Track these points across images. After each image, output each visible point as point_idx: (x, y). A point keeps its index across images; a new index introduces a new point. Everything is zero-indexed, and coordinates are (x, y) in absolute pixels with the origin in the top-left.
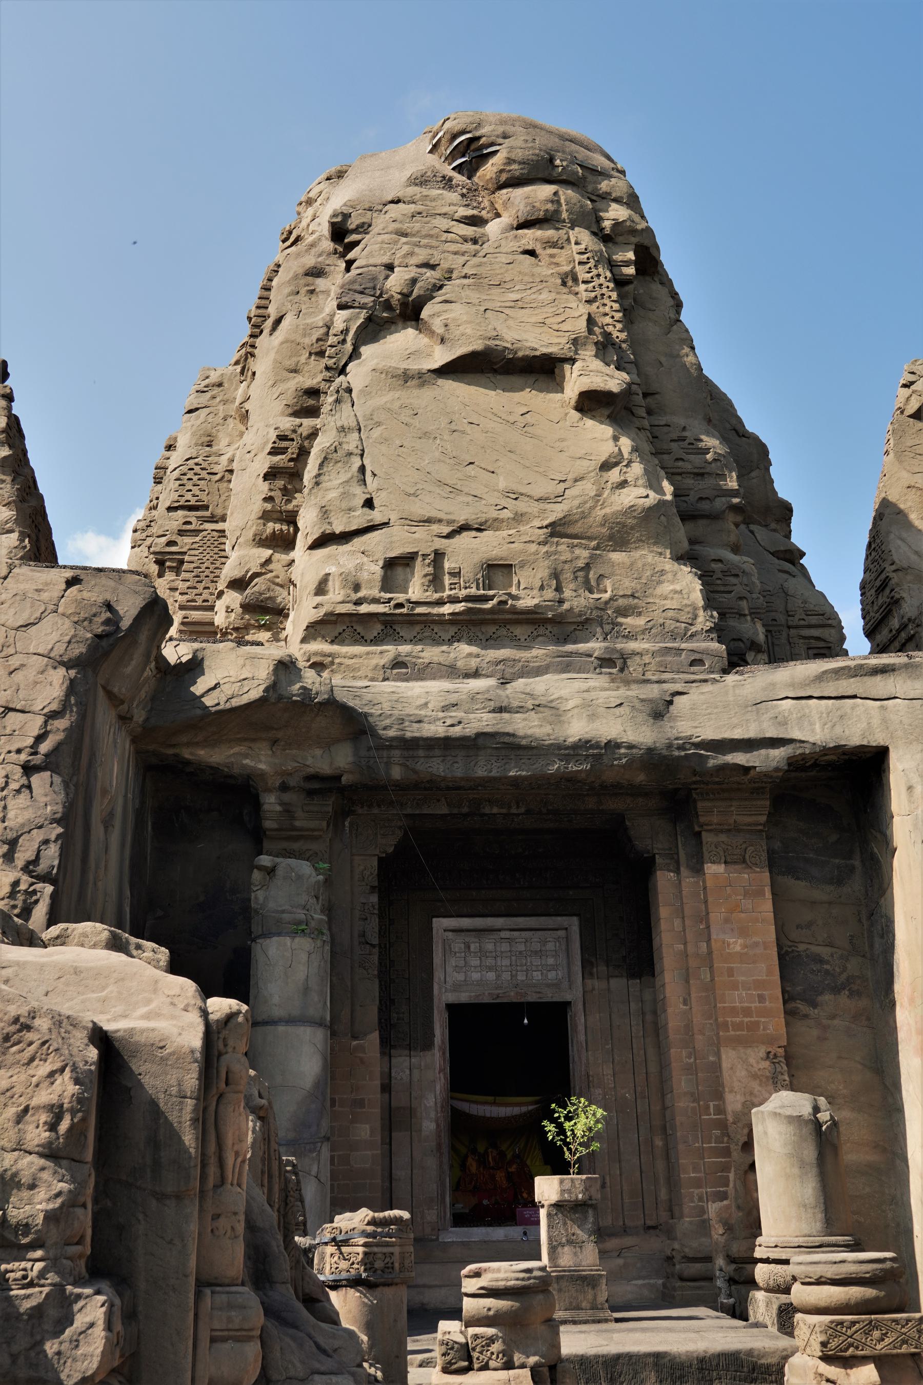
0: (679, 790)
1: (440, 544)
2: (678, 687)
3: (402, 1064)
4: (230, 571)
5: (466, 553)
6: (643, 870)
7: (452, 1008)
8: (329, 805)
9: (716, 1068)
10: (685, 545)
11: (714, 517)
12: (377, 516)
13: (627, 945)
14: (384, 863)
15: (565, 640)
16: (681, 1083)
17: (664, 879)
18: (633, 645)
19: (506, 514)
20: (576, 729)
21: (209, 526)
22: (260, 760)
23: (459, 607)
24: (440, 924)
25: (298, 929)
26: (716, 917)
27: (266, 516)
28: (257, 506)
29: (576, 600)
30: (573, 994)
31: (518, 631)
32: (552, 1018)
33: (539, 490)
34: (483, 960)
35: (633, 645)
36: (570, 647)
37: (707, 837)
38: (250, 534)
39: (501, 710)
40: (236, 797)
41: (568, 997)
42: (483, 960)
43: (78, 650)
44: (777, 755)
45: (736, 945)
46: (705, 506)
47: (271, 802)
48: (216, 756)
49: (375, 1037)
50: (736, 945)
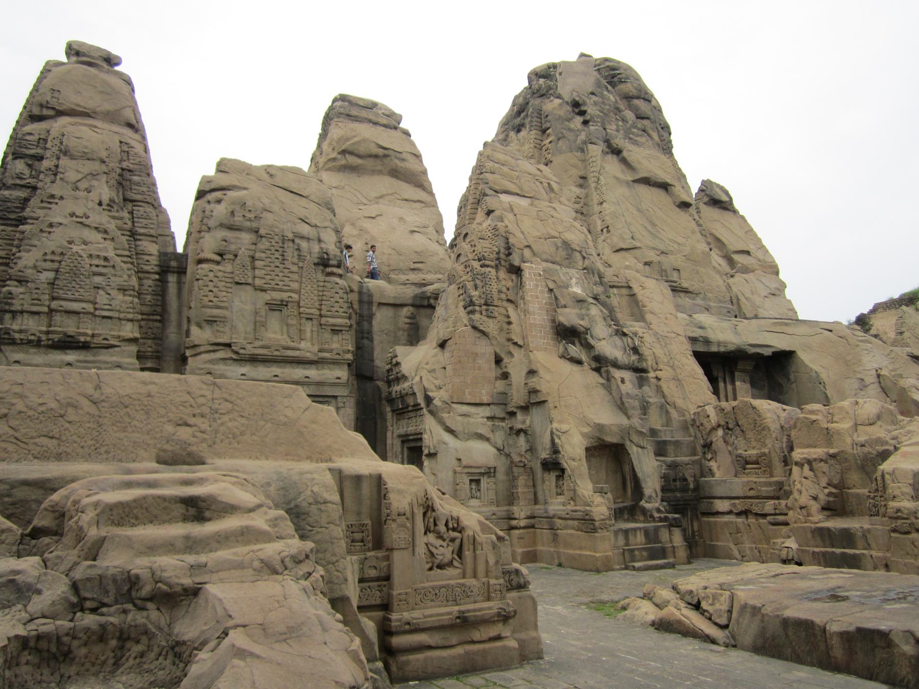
12: (638, 245)
15: (694, 299)
18: (712, 304)
31: (682, 295)
37: (737, 374)
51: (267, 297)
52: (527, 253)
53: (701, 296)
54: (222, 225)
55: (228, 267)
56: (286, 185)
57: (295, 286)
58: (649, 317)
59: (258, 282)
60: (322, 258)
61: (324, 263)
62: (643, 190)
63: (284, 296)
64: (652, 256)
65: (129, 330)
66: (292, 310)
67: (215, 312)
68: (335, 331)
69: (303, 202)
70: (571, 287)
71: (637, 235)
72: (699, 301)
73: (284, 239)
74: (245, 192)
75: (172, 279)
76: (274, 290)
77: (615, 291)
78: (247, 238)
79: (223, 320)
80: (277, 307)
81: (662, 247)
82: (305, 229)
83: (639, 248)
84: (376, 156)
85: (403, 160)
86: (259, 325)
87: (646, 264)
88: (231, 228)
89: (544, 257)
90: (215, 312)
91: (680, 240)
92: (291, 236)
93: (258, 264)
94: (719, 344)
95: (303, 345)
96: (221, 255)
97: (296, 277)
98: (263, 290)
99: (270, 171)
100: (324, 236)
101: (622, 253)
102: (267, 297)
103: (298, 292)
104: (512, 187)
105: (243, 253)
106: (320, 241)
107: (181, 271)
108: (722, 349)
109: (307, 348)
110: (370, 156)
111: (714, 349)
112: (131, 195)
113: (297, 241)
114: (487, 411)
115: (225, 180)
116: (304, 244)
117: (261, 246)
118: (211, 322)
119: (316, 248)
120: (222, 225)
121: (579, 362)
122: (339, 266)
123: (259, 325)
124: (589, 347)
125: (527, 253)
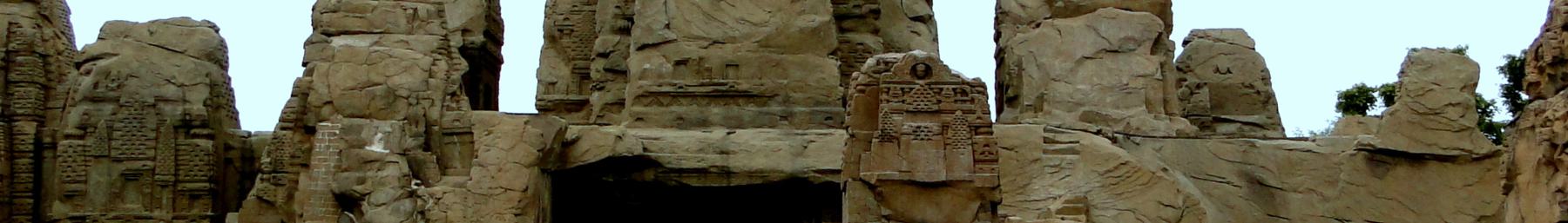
1: (703, 53)
2: (812, 137)
4: (598, 45)
5: (717, 55)
10: (836, 44)
12: (671, 35)
15: (765, 104)
18: (798, 109)
19: (737, 34)
20: (759, 163)
21: (587, 8)
23: (710, 88)
27: (616, 16)
28: (612, 10)
29: (768, 83)
31: (741, 101)
33: (755, 19)
35: (798, 109)
36: (765, 109)
38: (607, 27)
39: (722, 153)
43: (532, 159)
46: (857, 11)
51: (122, 167)
53: (779, 99)
54: (86, 99)
55: (89, 141)
56: (163, 42)
57: (151, 153)
59: (113, 153)
60: (184, 120)
61: (186, 125)
63: (138, 165)
64: (691, 50)
66: (147, 179)
67: (74, 186)
68: (194, 196)
69: (177, 59)
70: (371, 143)
71: (674, 23)
72: (775, 108)
73: (144, 105)
75: (48, 154)
76: (128, 159)
77: (455, 139)
78: (108, 108)
79: (83, 194)
80: (130, 177)
81: (716, 34)
82: (170, 91)
86: (117, 196)
87: (678, 63)
88: (94, 100)
89: (348, 112)
90: (74, 186)
91: (759, 16)
92: (152, 101)
93: (116, 134)
94: (750, 174)
95: (156, 213)
97: (152, 144)
98: (119, 161)
100: (191, 96)
101: (646, 52)
102: (122, 167)
103: (154, 159)
104: (352, 23)
105: (102, 124)
106: (185, 101)
107: (54, 146)
111: (735, 182)
112: (13, 76)
113: (161, 105)
115: (107, 47)
116: (167, 108)
117: (120, 116)
118: (68, 197)
119: (180, 109)
120: (86, 99)
122: (204, 125)
123: (117, 196)
125: (326, 110)
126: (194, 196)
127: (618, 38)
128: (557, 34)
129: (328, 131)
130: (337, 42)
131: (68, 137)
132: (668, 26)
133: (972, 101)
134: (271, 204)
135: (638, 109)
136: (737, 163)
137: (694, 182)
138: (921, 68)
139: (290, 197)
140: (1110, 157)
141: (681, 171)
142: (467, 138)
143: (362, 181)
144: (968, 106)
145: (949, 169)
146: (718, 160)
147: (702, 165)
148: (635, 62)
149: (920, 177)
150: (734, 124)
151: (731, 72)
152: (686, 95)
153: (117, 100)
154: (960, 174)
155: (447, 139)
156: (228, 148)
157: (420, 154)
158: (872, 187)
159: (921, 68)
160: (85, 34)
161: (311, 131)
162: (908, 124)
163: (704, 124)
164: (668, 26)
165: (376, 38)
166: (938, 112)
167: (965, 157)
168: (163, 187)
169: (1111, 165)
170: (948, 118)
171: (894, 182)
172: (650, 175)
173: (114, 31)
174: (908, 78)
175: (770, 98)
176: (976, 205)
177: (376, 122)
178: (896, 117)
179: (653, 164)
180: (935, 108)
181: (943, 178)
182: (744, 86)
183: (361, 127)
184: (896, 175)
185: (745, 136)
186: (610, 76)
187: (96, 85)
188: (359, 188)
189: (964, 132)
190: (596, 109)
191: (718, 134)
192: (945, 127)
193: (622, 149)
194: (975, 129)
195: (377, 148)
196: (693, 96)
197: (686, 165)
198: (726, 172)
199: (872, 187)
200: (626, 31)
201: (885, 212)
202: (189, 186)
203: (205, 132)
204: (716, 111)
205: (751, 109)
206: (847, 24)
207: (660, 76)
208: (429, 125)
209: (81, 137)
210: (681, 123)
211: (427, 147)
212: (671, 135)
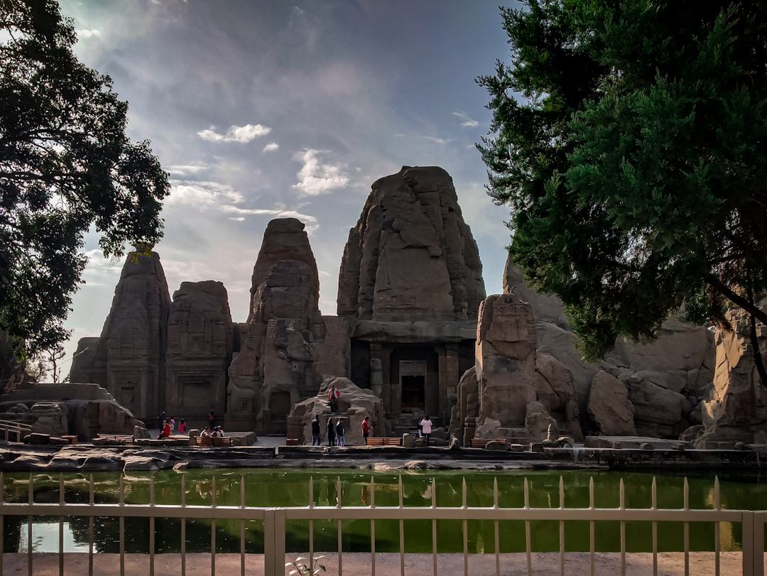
0: (442, 344)
3: (393, 387)
6: (437, 356)
7: (404, 378)
8: (381, 346)
9: (446, 391)
11: (459, 279)
13: (434, 367)
14: (391, 355)
16: (440, 392)
17: (440, 357)
20: (424, 334)
22: (370, 340)
24: (401, 361)
25: (379, 370)
26: (448, 365)
30: (425, 374)
31: (416, 311)
32: (421, 379)
34: (407, 369)
37: (448, 351)
40: (367, 344)
41: (423, 375)
42: (407, 369)
44: (461, 339)
45: (451, 370)
47: (371, 345)
48: (364, 339)
49: (389, 384)
50: (451, 370)
52: (271, 315)
58: (326, 337)
59: (189, 330)
62: (413, 251)
65: (144, 352)
74: (186, 296)
77: (318, 325)
78: (186, 314)
80: (196, 339)
83: (391, 289)
84: (283, 251)
85: (296, 251)
88: (181, 311)
94: (422, 337)
95: (205, 352)
96: (177, 321)
98: (190, 333)
99: (201, 284)
101: (381, 293)
108: (423, 341)
109: (208, 353)
110: (279, 252)
111: (419, 341)
114: (252, 378)
121: (283, 359)
124: (287, 352)
125: (271, 315)
126: (219, 346)
127: (368, 287)
128: (344, 286)
129: (272, 323)
130: (273, 289)
131: (171, 325)
132: (389, 283)
133: (527, 311)
134: (252, 350)
135: (378, 314)
136: (418, 334)
137: (401, 341)
138: (508, 299)
139: (259, 347)
140: (556, 331)
141: (396, 337)
142: (322, 325)
143: (286, 341)
144: (525, 313)
145: (519, 336)
146: (409, 333)
147: (404, 335)
148: (377, 297)
149: (509, 339)
150: (414, 319)
151: (413, 300)
152: (396, 309)
153: (189, 311)
154: (523, 338)
155: (315, 325)
156: (230, 329)
157: (306, 331)
158: (490, 343)
159: (508, 299)
160: (173, 288)
161: (266, 323)
162: (503, 320)
163: (402, 319)
164: (389, 283)
165: (286, 288)
166: (515, 316)
167: (525, 332)
168: (208, 343)
169: (558, 335)
170: (518, 318)
171: (498, 341)
172: (384, 338)
173: (186, 286)
174: (503, 303)
175: (428, 309)
176: (529, 349)
177: (290, 319)
178: (499, 317)
179: (387, 334)
180: (514, 314)
181: (516, 339)
182: (418, 305)
183: (284, 321)
184: (500, 339)
185: (420, 324)
186: (365, 301)
187: (181, 306)
188: (285, 343)
189: (524, 322)
190: (360, 315)
191: (408, 323)
192: (517, 322)
193: (375, 329)
194: (528, 322)
195: (291, 329)
196: (399, 309)
197: (399, 335)
198: (415, 338)
199: (490, 343)
200: (373, 285)
201: (495, 352)
202: (216, 342)
203: (222, 323)
204: (406, 315)
205: (420, 314)
206: (454, 282)
207: (387, 302)
208: (308, 320)
209: (177, 325)
210: (395, 319)
211: (308, 329)
212: (392, 323)
